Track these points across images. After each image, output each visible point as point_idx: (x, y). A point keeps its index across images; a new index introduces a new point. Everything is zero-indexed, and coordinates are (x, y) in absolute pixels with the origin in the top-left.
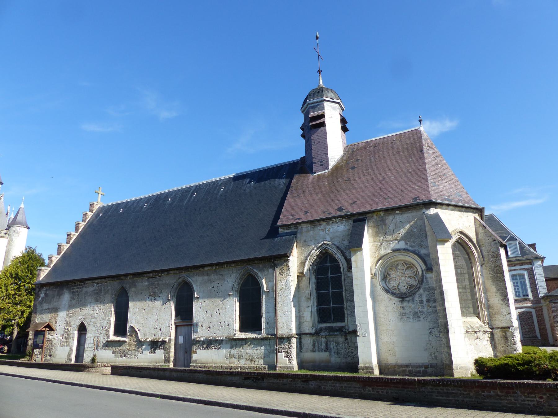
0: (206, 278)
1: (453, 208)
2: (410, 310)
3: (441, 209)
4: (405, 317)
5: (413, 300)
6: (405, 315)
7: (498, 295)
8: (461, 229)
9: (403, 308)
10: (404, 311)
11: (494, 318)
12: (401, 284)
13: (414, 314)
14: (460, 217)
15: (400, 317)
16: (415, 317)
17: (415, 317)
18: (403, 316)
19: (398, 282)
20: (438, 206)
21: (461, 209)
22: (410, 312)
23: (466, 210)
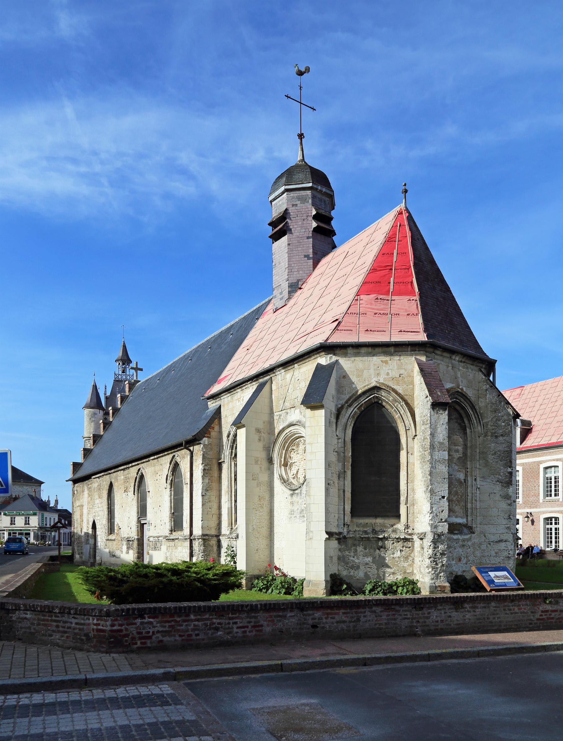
0: (153, 468)
1: (370, 350)
2: (298, 507)
3: (345, 355)
4: (293, 516)
5: (301, 493)
6: (293, 514)
7: (423, 483)
8: (382, 382)
9: (292, 503)
10: (293, 508)
11: (417, 519)
12: (300, 471)
13: (301, 513)
14: (386, 362)
15: (290, 516)
16: (300, 516)
17: (300, 516)
18: (292, 514)
19: (298, 468)
20: (337, 352)
21: (386, 349)
22: (298, 509)
23: (397, 349)
